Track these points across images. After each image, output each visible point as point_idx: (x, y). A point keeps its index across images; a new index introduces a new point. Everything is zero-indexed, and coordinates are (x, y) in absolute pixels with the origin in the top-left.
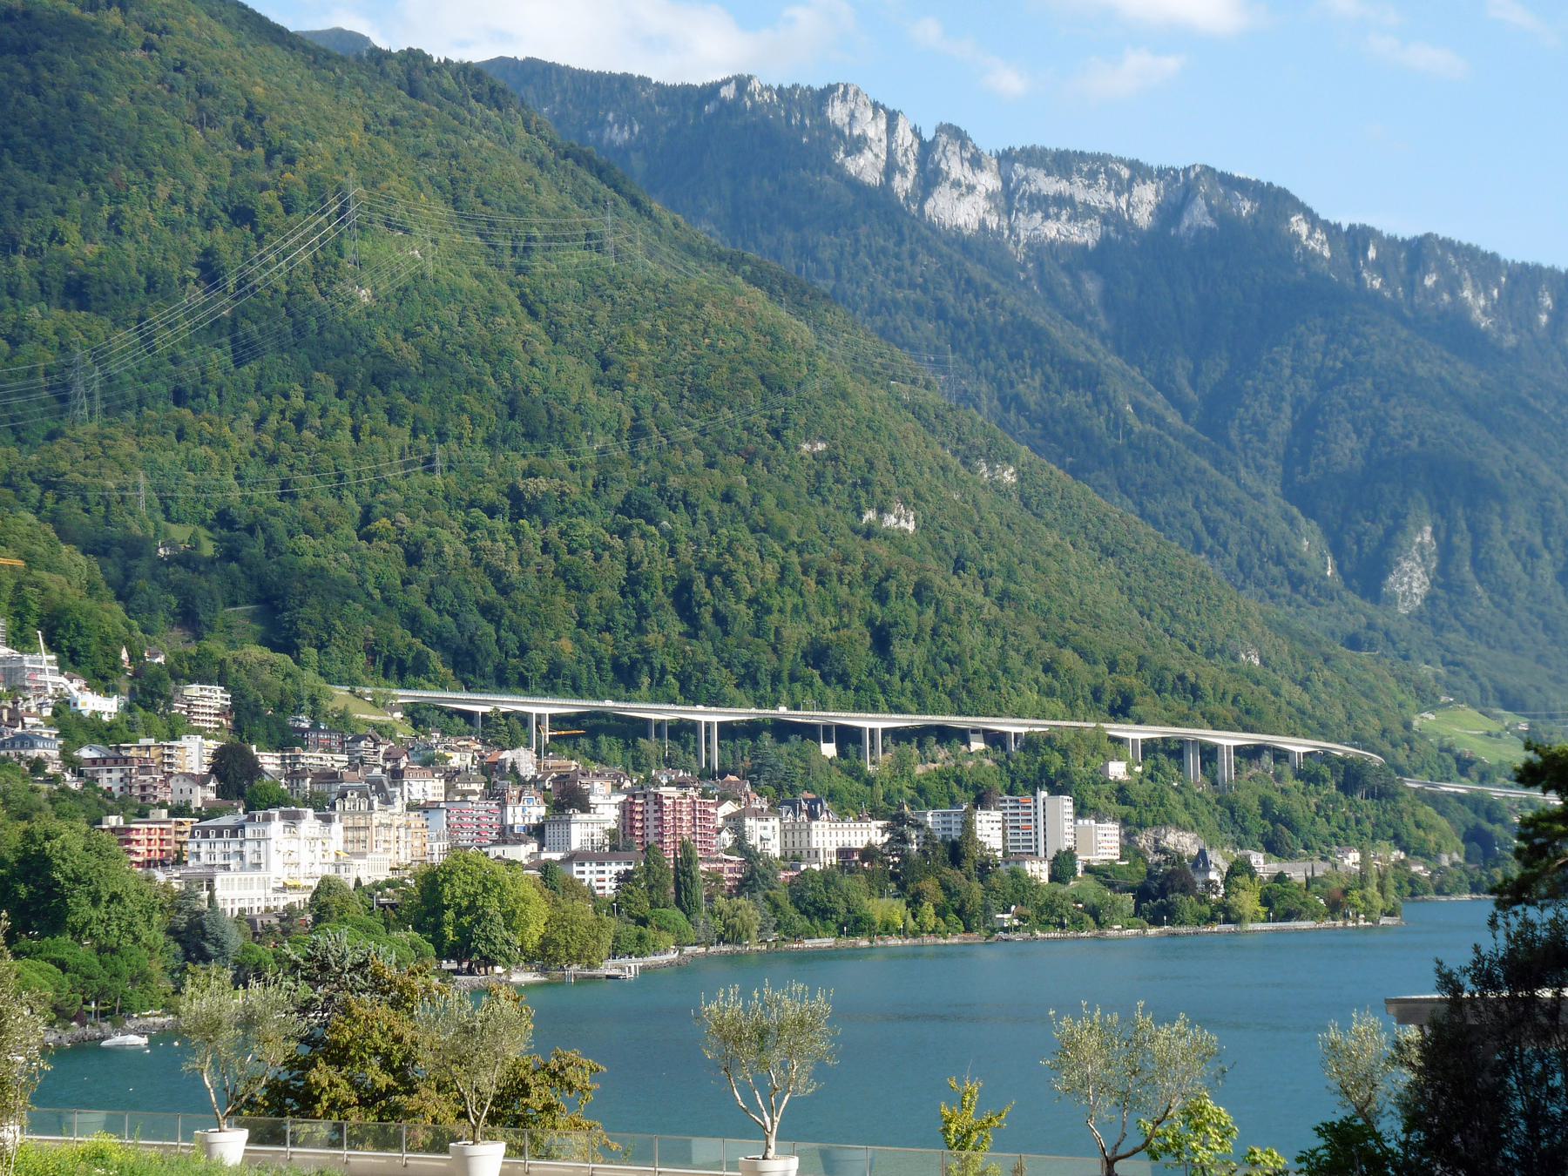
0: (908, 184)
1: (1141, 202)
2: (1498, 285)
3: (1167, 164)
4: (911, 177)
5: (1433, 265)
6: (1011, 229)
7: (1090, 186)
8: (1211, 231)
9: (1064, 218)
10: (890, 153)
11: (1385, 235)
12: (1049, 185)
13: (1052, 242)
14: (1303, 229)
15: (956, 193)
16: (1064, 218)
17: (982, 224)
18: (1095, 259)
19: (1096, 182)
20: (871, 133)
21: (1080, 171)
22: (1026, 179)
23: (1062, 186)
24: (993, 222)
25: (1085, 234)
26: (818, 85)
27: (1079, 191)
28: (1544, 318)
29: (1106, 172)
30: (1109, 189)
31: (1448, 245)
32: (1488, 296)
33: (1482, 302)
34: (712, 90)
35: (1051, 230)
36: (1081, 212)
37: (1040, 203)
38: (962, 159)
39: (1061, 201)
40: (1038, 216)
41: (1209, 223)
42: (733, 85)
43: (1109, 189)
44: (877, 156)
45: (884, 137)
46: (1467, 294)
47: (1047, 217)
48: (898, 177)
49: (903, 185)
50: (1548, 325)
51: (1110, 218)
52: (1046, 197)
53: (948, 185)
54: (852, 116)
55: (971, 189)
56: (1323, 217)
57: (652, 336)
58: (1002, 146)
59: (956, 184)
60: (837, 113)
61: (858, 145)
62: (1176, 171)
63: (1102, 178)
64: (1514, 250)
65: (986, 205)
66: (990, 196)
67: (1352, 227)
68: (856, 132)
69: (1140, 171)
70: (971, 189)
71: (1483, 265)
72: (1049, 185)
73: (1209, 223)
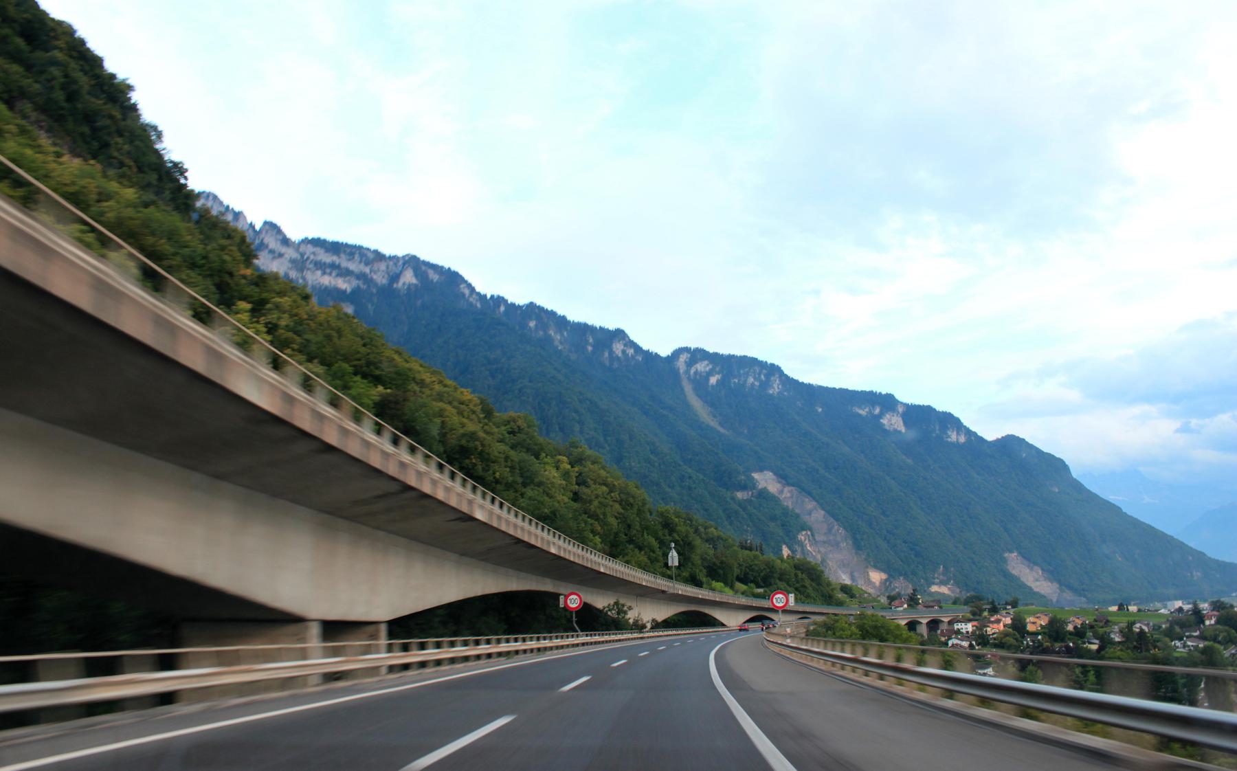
1: (379, 270)
2: (567, 330)
3: (393, 254)
5: (534, 317)
6: (304, 279)
7: (350, 260)
8: (416, 286)
9: (334, 274)
11: (509, 302)
12: (327, 258)
13: (326, 287)
14: (467, 292)
16: (334, 274)
18: (353, 297)
19: (354, 258)
21: (345, 252)
22: (314, 253)
23: (335, 258)
24: (293, 274)
25: (344, 285)
27: (345, 263)
28: (590, 348)
29: (360, 253)
30: (361, 262)
31: (541, 309)
32: (562, 335)
33: (559, 338)
35: (326, 280)
36: (346, 273)
37: (320, 266)
39: (333, 266)
40: (319, 273)
41: (414, 281)
43: (361, 262)
46: (552, 332)
47: (324, 273)
50: (592, 351)
51: (361, 276)
52: (325, 264)
53: (267, 251)
55: (281, 255)
56: (478, 290)
59: (272, 251)
62: (398, 258)
63: (357, 256)
64: (574, 316)
67: (492, 297)
69: (379, 256)
70: (281, 255)
71: (562, 322)
72: (327, 258)
73: (414, 281)
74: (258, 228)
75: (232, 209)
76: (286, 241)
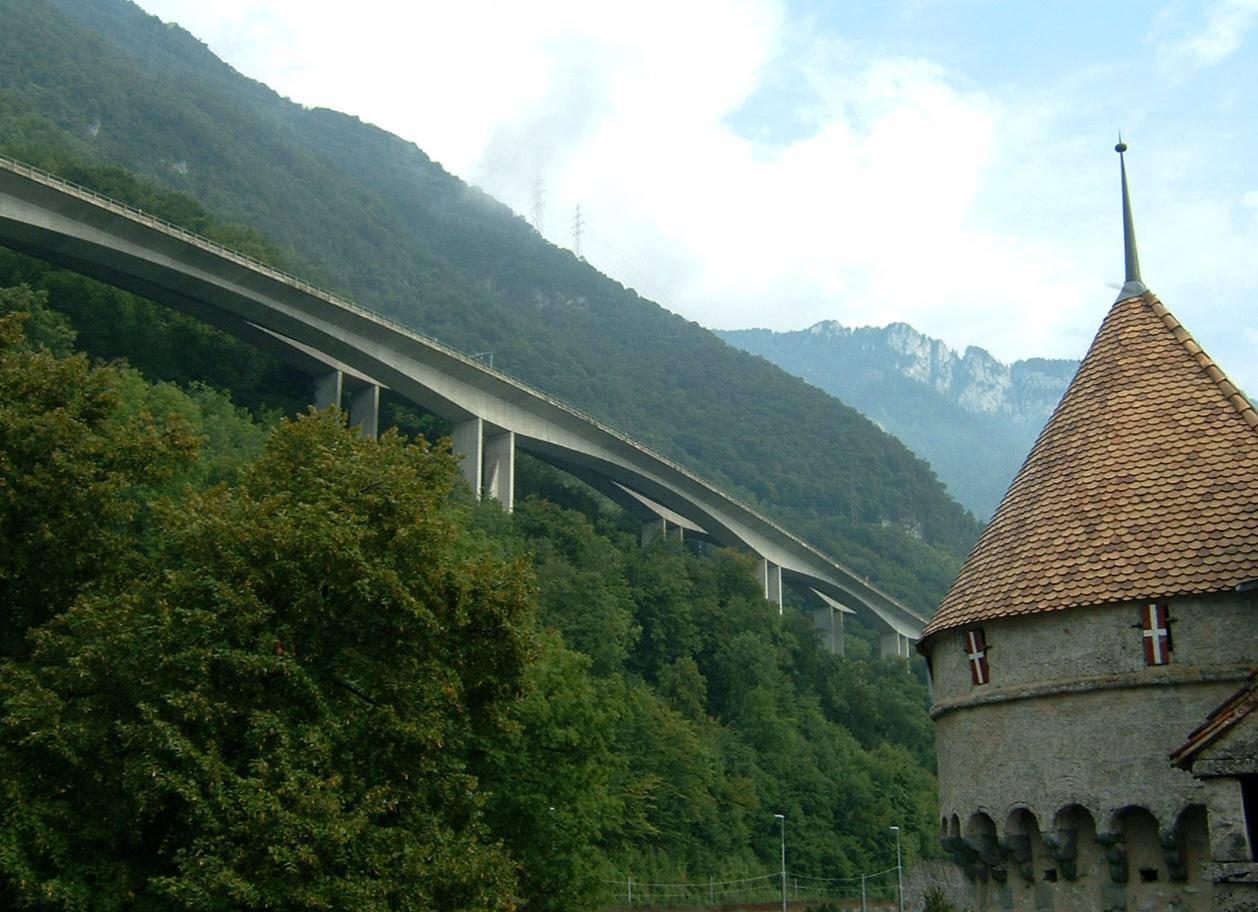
0: (947, 386)
4: (948, 381)
10: (934, 366)
15: (980, 389)
17: (1001, 408)
20: (920, 354)
26: (883, 326)
34: (807, 332)
38: (984, 368)
42: (820, 326)
44: (924, 369)
45: (929, 357)
48: (939, 381)
49: (943, 385)
53: (974, 385)
54: (905, 343)
57: (282, 660)
58: (1013, 360)
59: (981, 384)
60: (895, 341)
61: (911, 360)
65: (1000, 397)
66: (1006, 392)
68: (908, 353)
74: (961, 355)
75: (929, 338)
76: (996, 368)
